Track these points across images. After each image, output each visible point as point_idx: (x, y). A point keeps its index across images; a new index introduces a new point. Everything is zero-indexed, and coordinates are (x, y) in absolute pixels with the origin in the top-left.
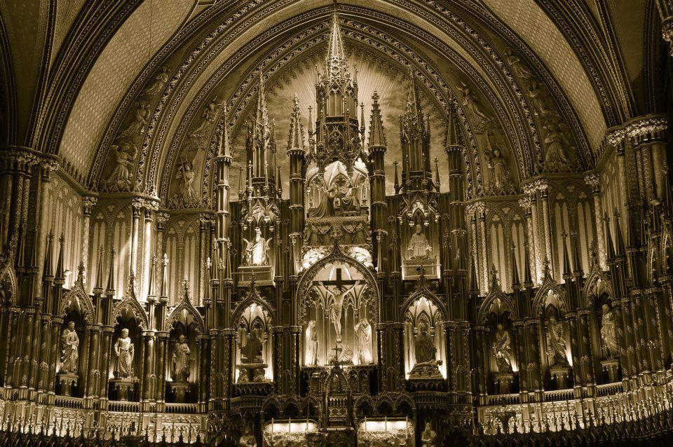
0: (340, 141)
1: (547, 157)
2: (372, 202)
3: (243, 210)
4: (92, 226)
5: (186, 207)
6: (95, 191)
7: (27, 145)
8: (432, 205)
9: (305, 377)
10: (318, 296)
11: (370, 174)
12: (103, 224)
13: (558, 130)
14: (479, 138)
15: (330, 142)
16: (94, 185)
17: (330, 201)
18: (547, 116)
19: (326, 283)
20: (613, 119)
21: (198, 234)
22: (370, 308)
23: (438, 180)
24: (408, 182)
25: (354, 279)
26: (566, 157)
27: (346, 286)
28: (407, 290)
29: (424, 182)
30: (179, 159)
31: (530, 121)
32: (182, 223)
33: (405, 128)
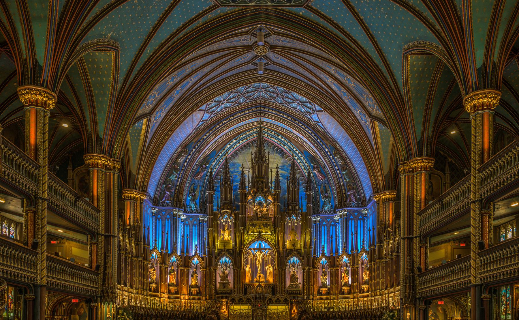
0: (262, 188)
1: (348, 200)
2: (274, 215)
3: (219, 215)
4: (156, 220)
5: (193, 212)
6: (156, 205)
7: (135, 189)
8: (299, 217)
9: (246, 289)
10: (250, 254)
11: (274, 203)
12: (161, 220)
13: (353, 189)
14: (319, 187)
15: (258, 189)
16: (156, 203)
17: (257, 214)
18: (349, 182)
19: (254, 249)
20: (376, 191)
21: (198, 224)
22: (272, 260)
23: (302, 207)
24: (290, 208)
25: (266, 248)
26: (355, 201)
27: (263, 251)
28: (289, 253)
29: (297, 208)
30: (189, 191)
31: (342, 184)
32: (191, 219)
33: (289, 183)
